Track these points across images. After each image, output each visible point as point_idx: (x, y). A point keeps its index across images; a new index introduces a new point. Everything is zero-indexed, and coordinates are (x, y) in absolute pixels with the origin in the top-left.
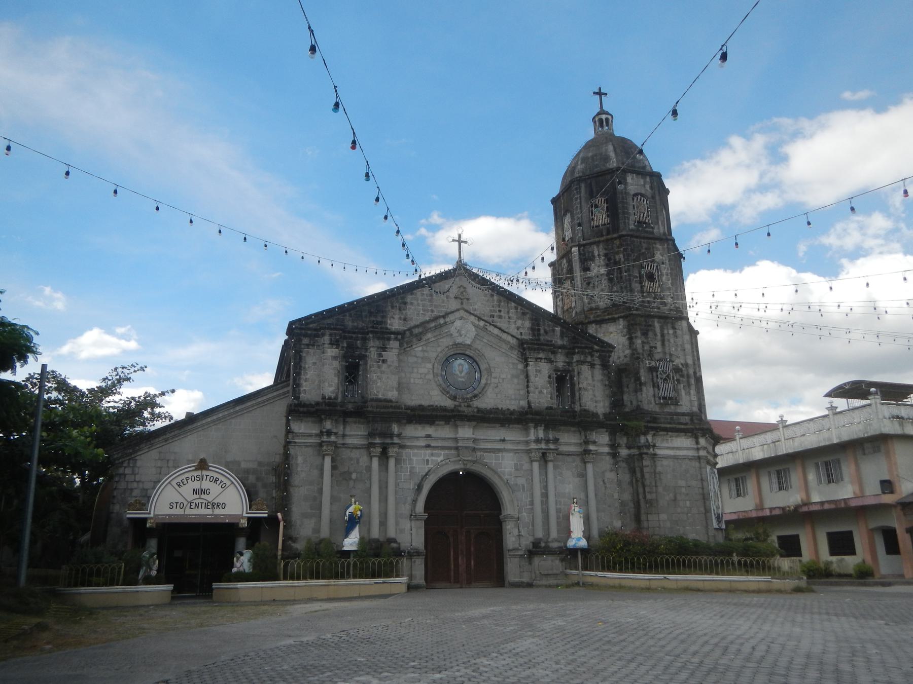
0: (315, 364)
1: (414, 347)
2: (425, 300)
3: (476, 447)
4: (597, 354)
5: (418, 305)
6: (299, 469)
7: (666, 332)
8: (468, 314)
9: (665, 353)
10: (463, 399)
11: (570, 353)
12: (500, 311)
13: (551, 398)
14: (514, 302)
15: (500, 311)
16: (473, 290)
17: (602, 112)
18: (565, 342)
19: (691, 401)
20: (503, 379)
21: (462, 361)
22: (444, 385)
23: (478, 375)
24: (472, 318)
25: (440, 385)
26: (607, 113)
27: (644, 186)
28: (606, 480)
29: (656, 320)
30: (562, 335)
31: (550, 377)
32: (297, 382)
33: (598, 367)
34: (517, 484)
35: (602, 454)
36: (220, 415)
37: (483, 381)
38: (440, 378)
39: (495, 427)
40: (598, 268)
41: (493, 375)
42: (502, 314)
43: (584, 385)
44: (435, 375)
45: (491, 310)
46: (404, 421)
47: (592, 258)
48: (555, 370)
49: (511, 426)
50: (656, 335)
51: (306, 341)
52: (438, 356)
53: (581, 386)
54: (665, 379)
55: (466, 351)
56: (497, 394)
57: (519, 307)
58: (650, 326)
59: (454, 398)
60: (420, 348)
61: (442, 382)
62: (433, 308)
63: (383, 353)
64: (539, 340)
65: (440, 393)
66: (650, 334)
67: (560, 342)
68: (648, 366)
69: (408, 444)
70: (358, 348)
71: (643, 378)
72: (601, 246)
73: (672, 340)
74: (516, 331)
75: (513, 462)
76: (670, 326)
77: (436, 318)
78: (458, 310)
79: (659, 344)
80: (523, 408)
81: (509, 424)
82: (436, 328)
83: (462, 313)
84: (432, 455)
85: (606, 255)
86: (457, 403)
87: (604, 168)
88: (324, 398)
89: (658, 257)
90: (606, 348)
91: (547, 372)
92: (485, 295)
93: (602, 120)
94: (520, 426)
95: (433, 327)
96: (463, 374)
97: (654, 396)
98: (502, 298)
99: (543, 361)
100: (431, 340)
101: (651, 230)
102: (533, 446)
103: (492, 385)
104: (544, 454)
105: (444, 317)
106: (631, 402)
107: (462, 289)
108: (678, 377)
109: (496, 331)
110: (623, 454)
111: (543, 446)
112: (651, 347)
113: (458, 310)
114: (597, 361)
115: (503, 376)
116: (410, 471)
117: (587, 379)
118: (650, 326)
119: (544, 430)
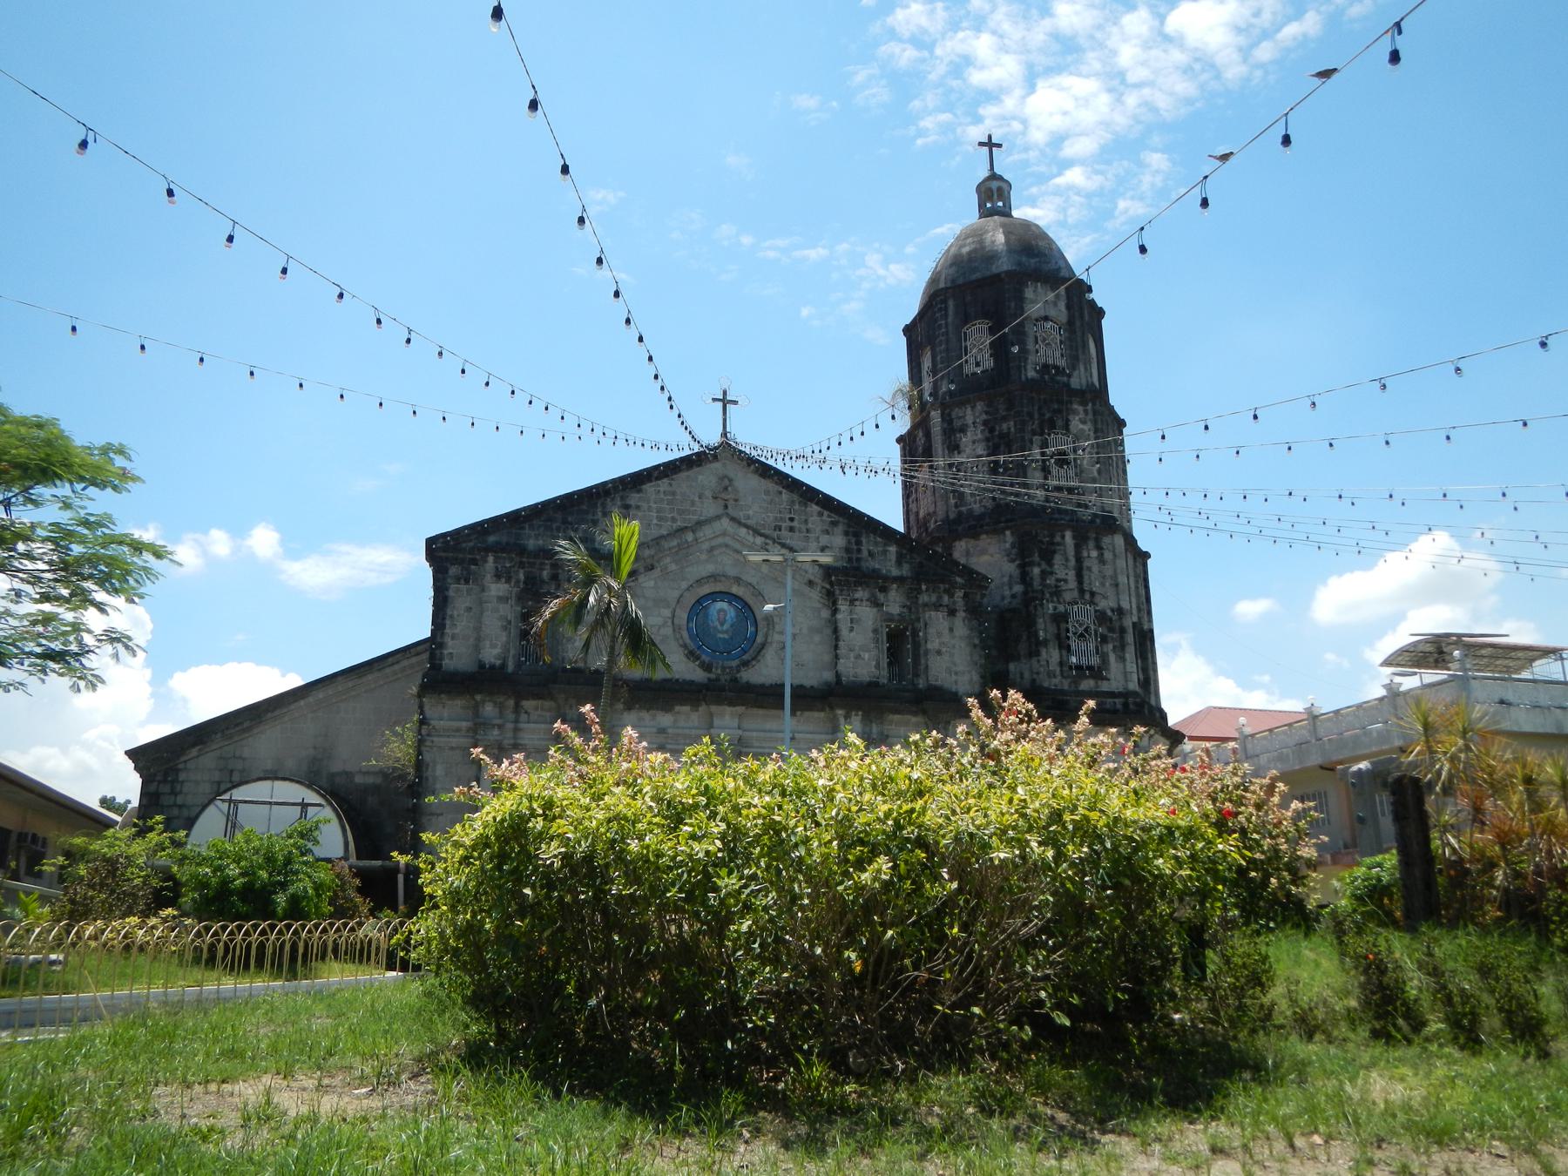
0: (469, 609)
2: (662, 500)
5: (650, 509)
7: (1085, 554)
8: (736, 526)
9: (1082, 591)
10: (724, 668)
11: (913, 594)
12: (792, 520)
13: (878, 666)
14: (817, 504)
15: (792, 520)
16: (748, 483)
17: (994, 176)
18: (906, 570)
19: (1125, 673)
21: (724, 605)
22: (692, 646)
23: (751, 629)
24: (743, 531)
25: (685, 646)
26: (1001, 178)
27: (1055, 304)
29: (1068, 535)
30: (899, 563)
31: (875, 631)
32: (439, 640)
33: (961, 614)
36: (321, 695)
37: (759, 639)
38: (685, 634)
40: (973, 448)
42: (795, 524)
43: (933, 645)
44: (677, 629)
45: (776, 518)
47: (963, 430)
48: (885, 620)
49: (807, 714)
50: (1067, 560)
51: (454, 570)
52: (681, 596)
53: (929, 646)
54: (1082, 635)
57: (826, 513)
58: (1058, 544)
59: (707, 667)
60: (652, 583)
61: (688, 641)
62: (675, 514)
64: (858, 569)
65: (685, 659)
66: (1058, 559)
67: (895, 572)
68: (1051, 611)
70: (543, 582)
71: (1041, 633)
72: (980, 406)
73: (1095, 569)
76: (1091, 544)
77: (682, 530)
78: (718, 517)
79: (1071, 575)
80: (827, 684)
81: (802, 710)
83: (725, 522)
85: (985, 423)
86: (713, 676)
87: (988, 273)
88: (481, 665)
89: (1076, 424)
90: (975, 580)
92: (767, 493)
93: (994, 194)
94: (822, 714)
96: (725, 627)
97: (1061, 664)
98: (796, 497)
99: (864, 603)
101: (1065, 379)
103: (774, 645)
106: (1022, 675)
107: (726, 482)
108: (1106, 632)
112: (1058, 580)
117: (939, 634)
118: (1058, 544)
119: (862, 721)
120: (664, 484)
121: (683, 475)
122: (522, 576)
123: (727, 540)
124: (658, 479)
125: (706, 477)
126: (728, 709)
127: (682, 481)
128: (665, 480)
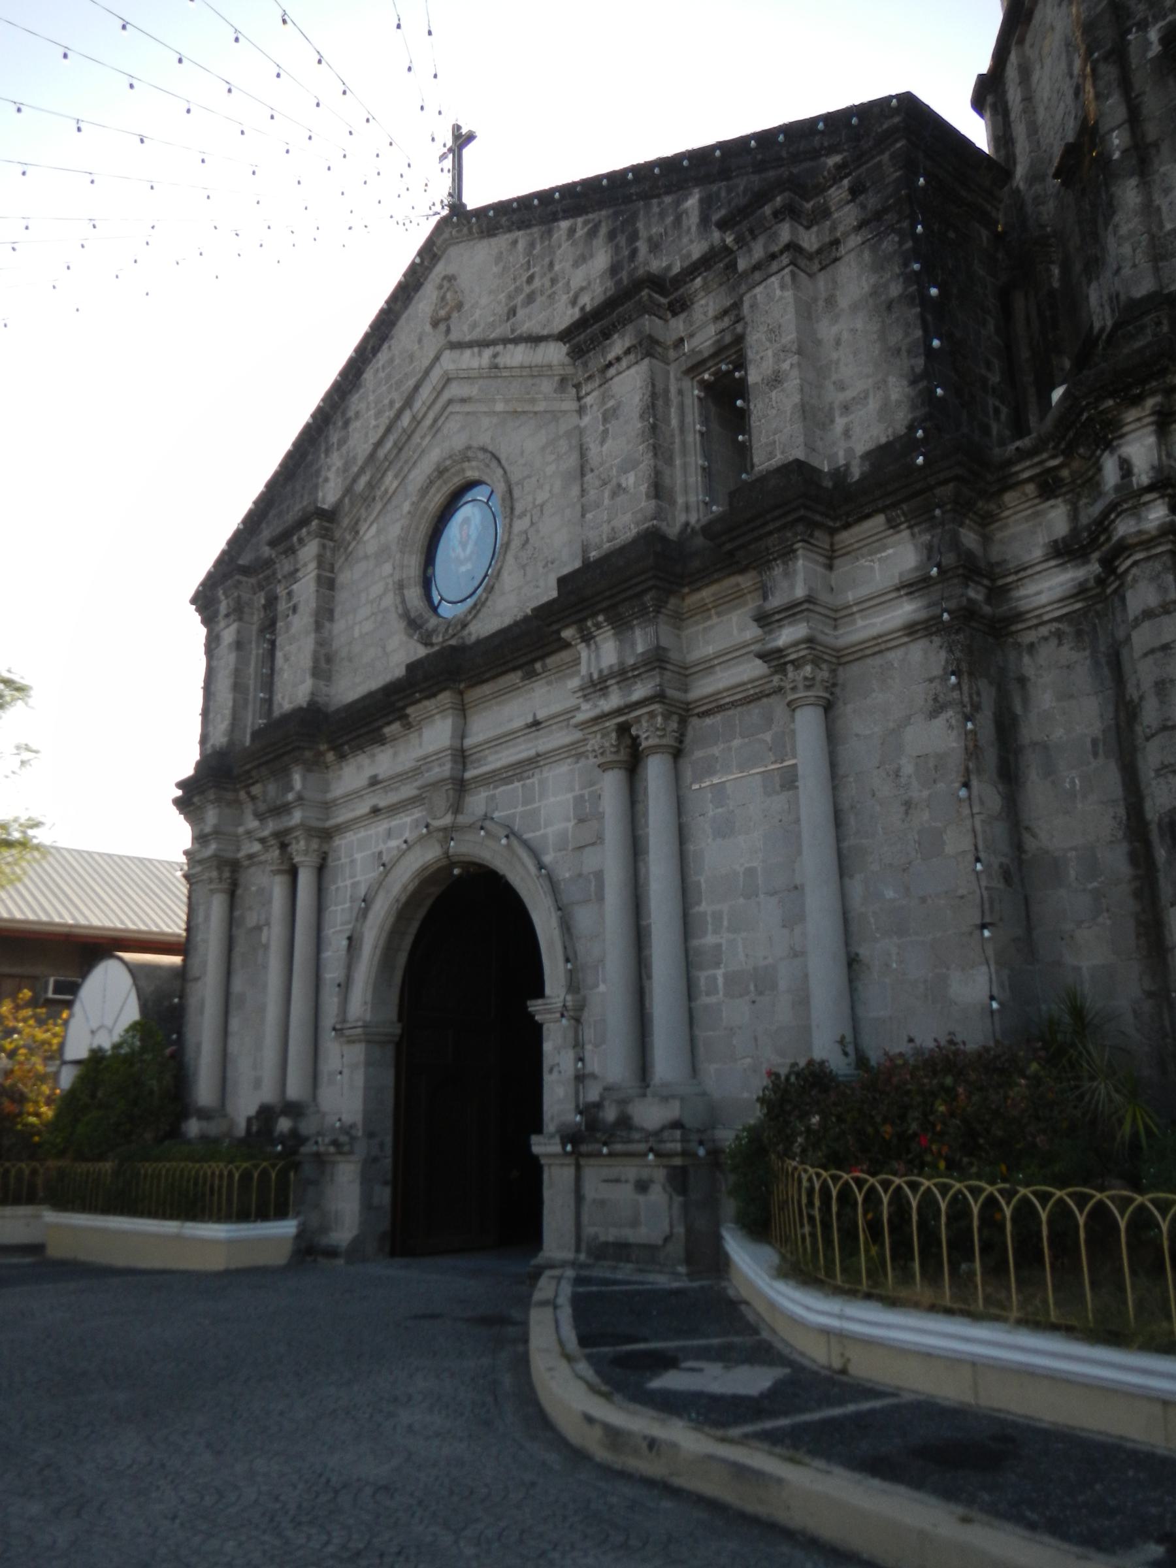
1: (361, 533)
3: (468, 775)
4: (837, 193)
6: (199, 939)
13: (659, 490)
15: (530, 279)
20: (542, 506)
28: (908, 769)
33: (854, 241)
34: (580, 875)
35: (879, 645)
38: (414, 594)
39: (513, 689)
41: (519, 508)
42: (537, 283)
46: (330, 756)
49: (551, 661)
55: (463, 470)
56: (524, 567)
57: (580, 220)
63: (295, 587)
69: (340, 820)
74: (570, 312)
75: (570, 796)
78: (437, 358)
81: (542, 658)
82: (399, 448)
83: (450, 362)
84: (389, 834)
91: (637, 399)
95: (390, 451)
96: (468, 551)
100: (391, 491)
102: (587, 711)
104: (623, 730)
105: (408, 402)
109: (517, 355)
110: (1044, 599)
111: (614, 700)
113: (437, 358)
114: (847, 216)
115: (541, 497)
116: (351, 897)
117: (774, 332)
119: (615, 634)
120: (383, 357)
121: (405, 316)
122: (263, 601)
123: (454, 390)
124: (375, 351)
125: (425, 303)
126: (429, 704)
127: (404, 337)
128: (385, 346)
